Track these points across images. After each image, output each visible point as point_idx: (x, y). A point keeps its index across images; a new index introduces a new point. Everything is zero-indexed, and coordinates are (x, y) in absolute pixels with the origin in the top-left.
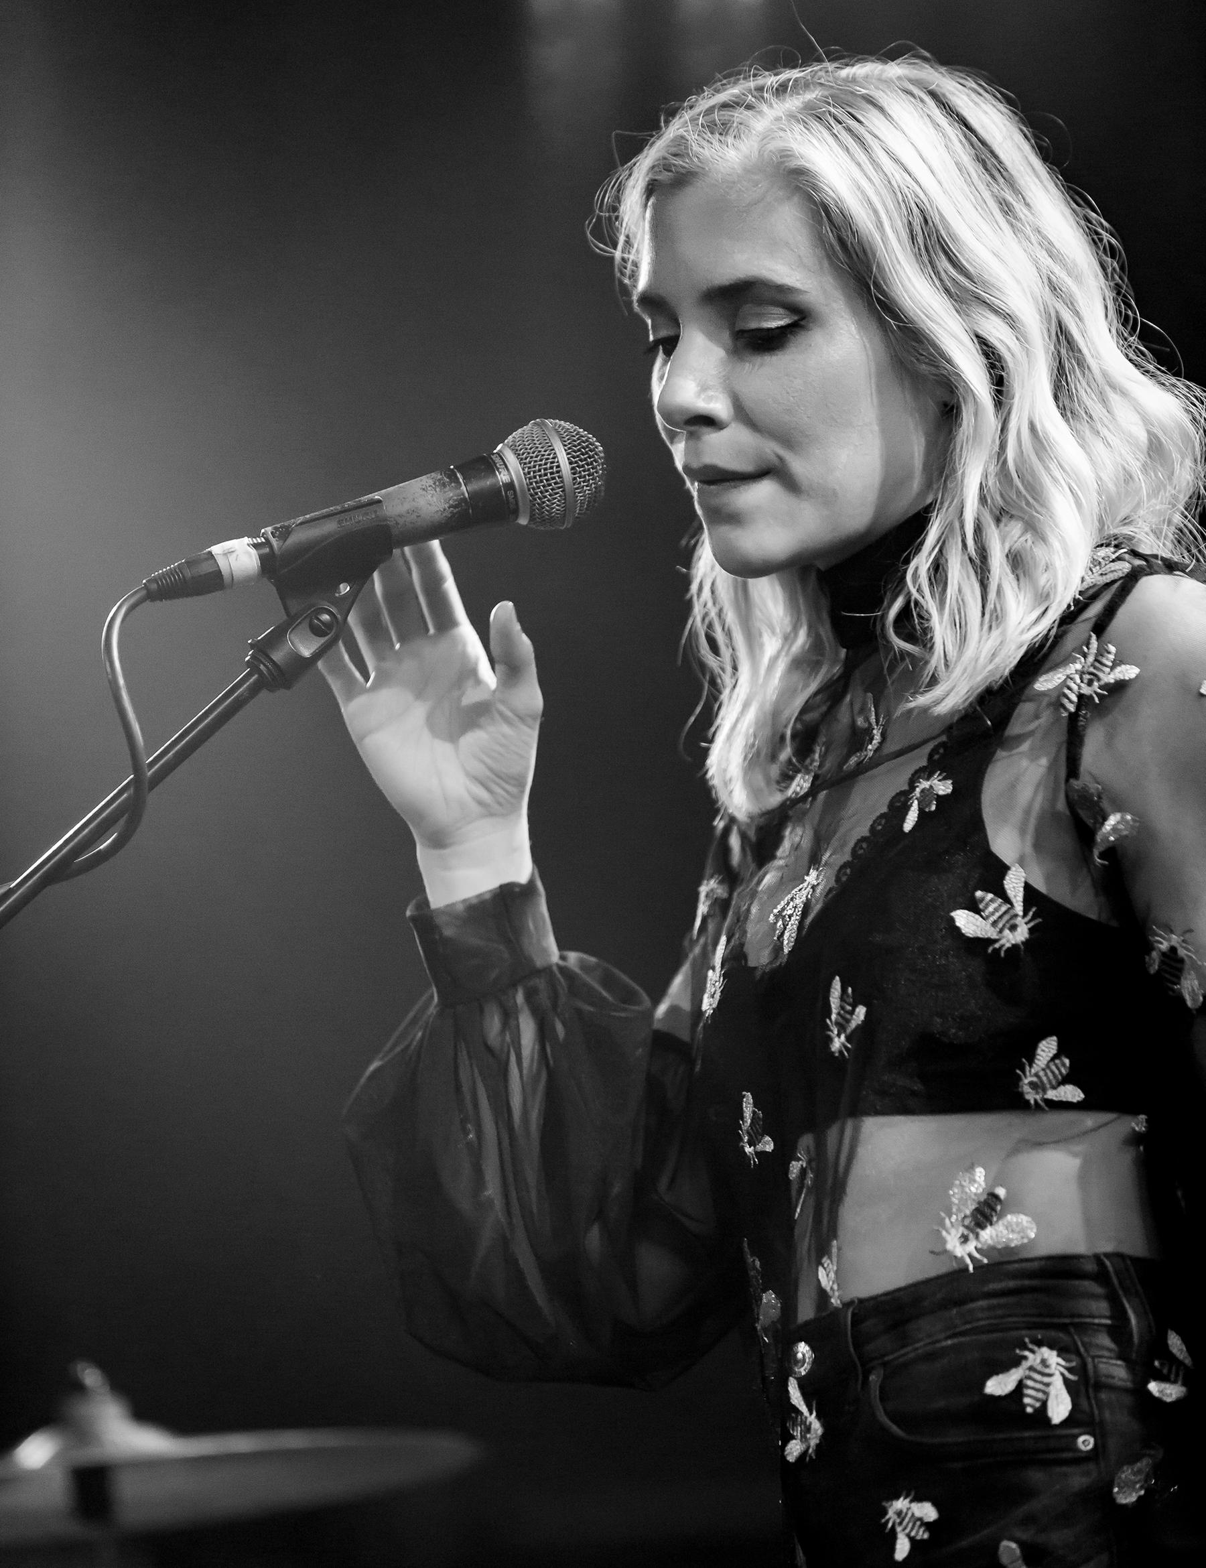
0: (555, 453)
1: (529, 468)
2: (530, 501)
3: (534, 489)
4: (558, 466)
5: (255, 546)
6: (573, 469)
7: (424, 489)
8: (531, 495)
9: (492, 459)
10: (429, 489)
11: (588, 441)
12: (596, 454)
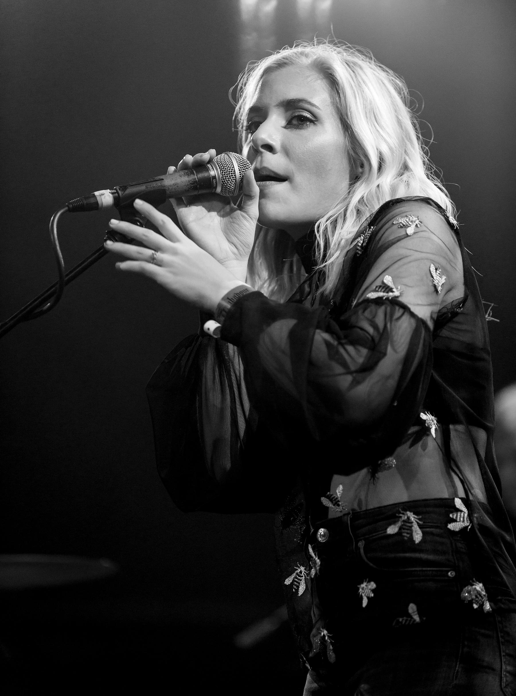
0: (233, 166)
1: (223, 171)
2: (222, 184)
3: (224, 179)
4: (234, 171)
5: (112, 193)
6: (240, 172)
7: (180, 176)
8: (222, 182)
9: (208, 166)
10: (182, 176)
11: (246, 162)
12: (249, 167)
